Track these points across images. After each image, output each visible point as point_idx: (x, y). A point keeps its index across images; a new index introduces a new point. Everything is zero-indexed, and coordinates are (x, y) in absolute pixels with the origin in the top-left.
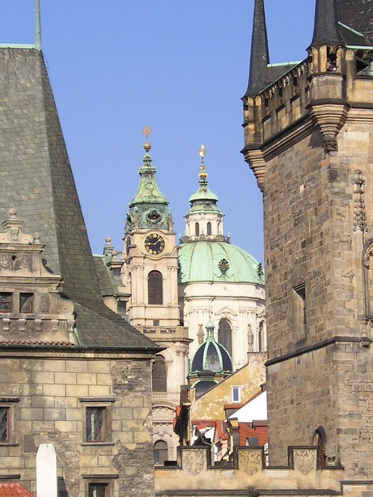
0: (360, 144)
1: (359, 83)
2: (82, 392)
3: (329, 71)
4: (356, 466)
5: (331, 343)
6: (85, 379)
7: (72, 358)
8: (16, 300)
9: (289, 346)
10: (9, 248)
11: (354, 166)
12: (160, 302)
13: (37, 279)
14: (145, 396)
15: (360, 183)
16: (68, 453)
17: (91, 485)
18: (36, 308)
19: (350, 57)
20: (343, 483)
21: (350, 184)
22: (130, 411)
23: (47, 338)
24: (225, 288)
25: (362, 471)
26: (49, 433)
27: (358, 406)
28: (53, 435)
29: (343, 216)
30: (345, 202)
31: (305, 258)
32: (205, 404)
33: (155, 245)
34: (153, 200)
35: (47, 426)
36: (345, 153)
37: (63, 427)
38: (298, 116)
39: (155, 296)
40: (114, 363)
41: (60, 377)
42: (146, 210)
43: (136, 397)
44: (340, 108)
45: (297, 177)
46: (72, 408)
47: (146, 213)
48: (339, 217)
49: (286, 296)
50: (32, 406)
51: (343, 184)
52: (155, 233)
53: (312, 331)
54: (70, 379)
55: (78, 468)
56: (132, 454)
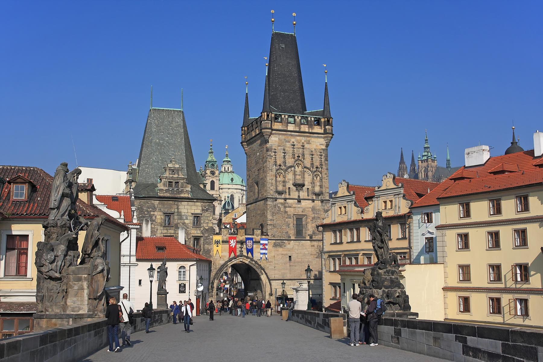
0: (275, 141)
3: (267, 120)
5: (266, 199)
6: (194, 208)
8: (174, 184)
11: (273, 148)
15: (275, 152)
19: (273, 116)
23: (182, 195)
25: (274, 236)
33: (213, 173)
37: (187, 221)
39: (212, 188)
44: (270, 130)
50: (178, 215)
53: (260, 196)
54: (189, 208)
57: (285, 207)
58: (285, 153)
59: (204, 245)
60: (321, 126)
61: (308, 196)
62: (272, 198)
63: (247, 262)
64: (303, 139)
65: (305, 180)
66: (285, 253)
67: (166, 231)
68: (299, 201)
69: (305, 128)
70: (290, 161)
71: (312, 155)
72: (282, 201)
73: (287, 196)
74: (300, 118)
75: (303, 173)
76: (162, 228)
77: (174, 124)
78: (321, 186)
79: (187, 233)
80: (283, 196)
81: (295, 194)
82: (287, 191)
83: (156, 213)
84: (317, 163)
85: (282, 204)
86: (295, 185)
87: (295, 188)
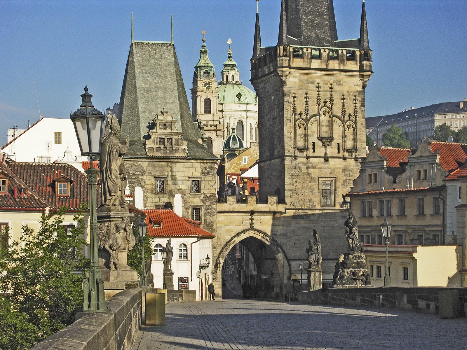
0: (295, 82)
1: (295, 59)
2: (190, 175)
4: (291, 203)
6: (191, 170)
7: (187, 162)
9: (267, 157)
10: (163, 121)
11: (292, 91)
12: (210, 112)
13: (173, 133)
14: (213, 177)
15: (294, 97)
16: (185, 197)
17: (193, 209)
18: (173, 144)
19: (291, 50)
20: (286, 209)
21: (291, 98)
22: (208, 182)
23: (177, 155)
24: (240, 106)
25: (293, 205)
26: (178, 189)
27: (292, 181)
28: (180, 190)
29: (288, 110)
30: (289, 105)
31: (273, 124)
32: (231, 164)
34: (206, 65)
35: (177, 187)
36: (289, 86)
37: (183, 187)
38: (272, 70)
39: (208, 110)
40: (202, 164)
41: (182, 169)
42: (203, 70)
43: (210, 177)
45: (271, 93)
46: (186, 180)
47: (203, 71)
48: (287, 110)
49: (266, 137)
51: (288, 98)
52: (207, 81)
54: (186, 170)
55: (189, 202)
56: (208, 198)
57: (308, 168)
58: (306, 98)
59: (205, 216)
60: (356, 61)
61: (339, 152)
62: (291, 156)
63: (259, 237)
64: (331, 79)
65: (334, 132)
66: (308, 225)
67: (158, 200)
68: (326, 159)
69: (334, 64)
70: (313, 109)
71: (343, 99)
72: (304, 160)
73: (310, 153)
74: (327, 51)
75: (331, 124)
76: (153, 196)
77: (164, 62)
78: (355, 140)
79: (184, 202)
80: (305, 154)
81: (320, 151)
82: (311, 147)
83: (145, 177)
84: (350, 110)
85: (304, 164)
86: (320, 139)
87: (320, 143)
